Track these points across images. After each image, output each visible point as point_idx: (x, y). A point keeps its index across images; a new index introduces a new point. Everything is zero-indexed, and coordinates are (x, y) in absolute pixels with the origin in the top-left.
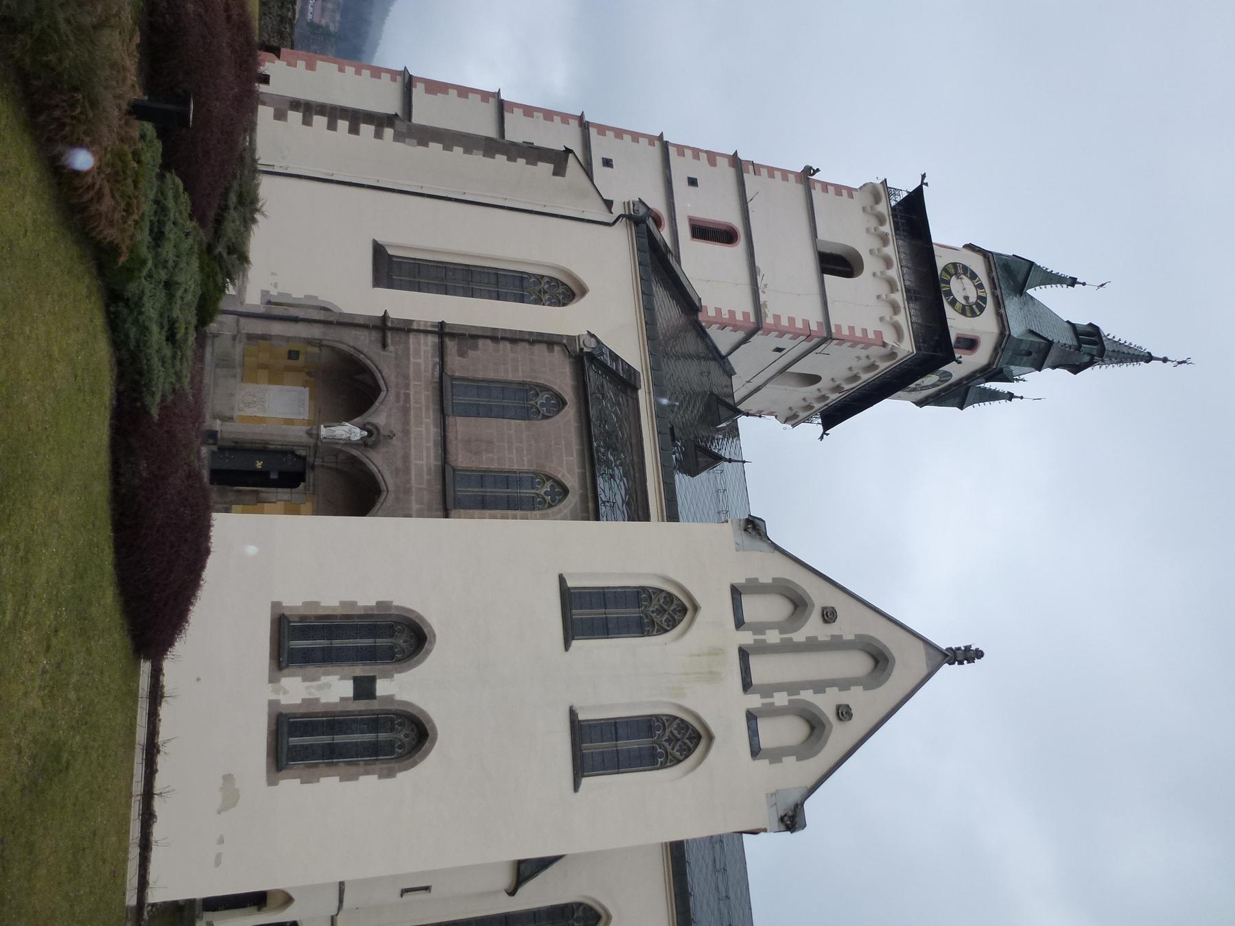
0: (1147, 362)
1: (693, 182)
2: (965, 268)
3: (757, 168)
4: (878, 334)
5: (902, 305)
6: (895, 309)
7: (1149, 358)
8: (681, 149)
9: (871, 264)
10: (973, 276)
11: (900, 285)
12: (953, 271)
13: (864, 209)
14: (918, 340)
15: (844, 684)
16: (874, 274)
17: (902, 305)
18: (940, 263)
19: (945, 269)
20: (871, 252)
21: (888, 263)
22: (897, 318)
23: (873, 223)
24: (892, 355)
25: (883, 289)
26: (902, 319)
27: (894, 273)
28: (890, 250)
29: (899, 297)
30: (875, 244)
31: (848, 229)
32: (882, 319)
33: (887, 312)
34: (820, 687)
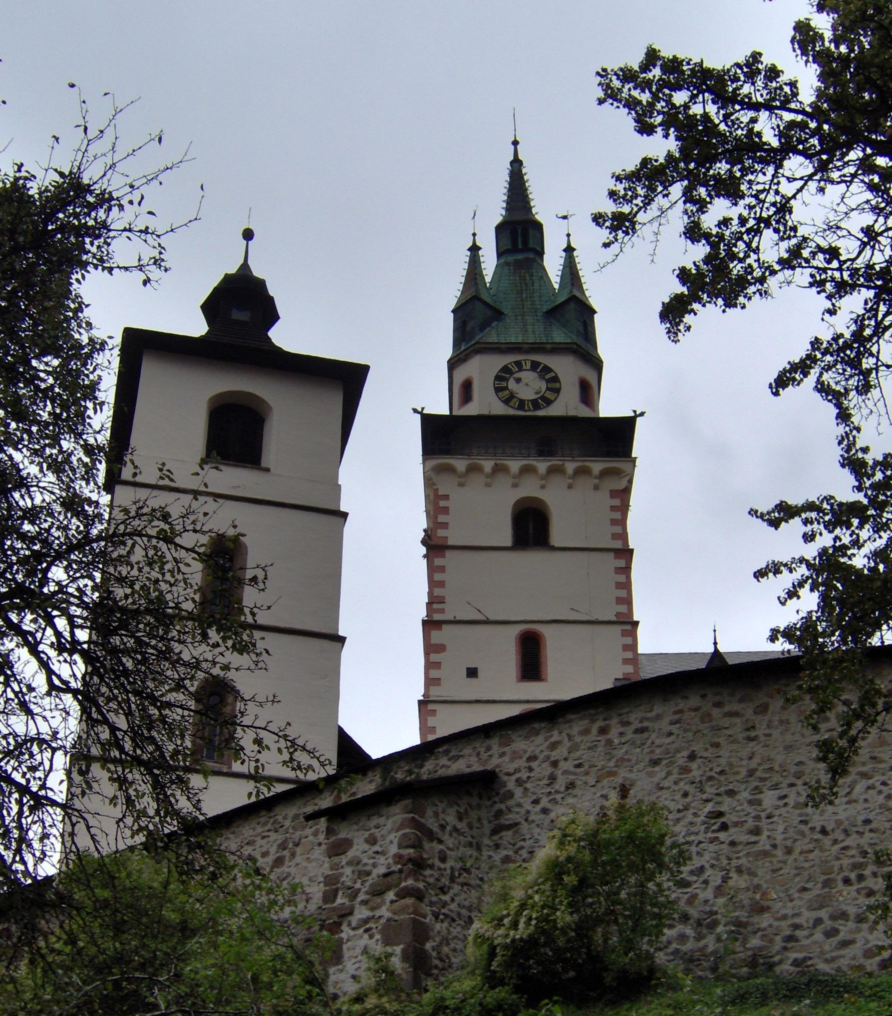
0: (520, 163)
1: (472, 673)
2: (498, 378)
3: (433, 602)
5: (581, 464)
6: (582, 472)
7: (516, 163)
8: (430, 682)
9: (529, 489)
10: (506, 369)
11: (555, 462)
12: (506, 393)
13: (461, 485)
16: (543, 487)
17: (581, 464)
18: (499, 409)
19: (507, 402)
20: (515, 486)
21: (527, 470)
23: (477, 480)
30: (503, 482)
31: (488, 509)
32: (596, 488)
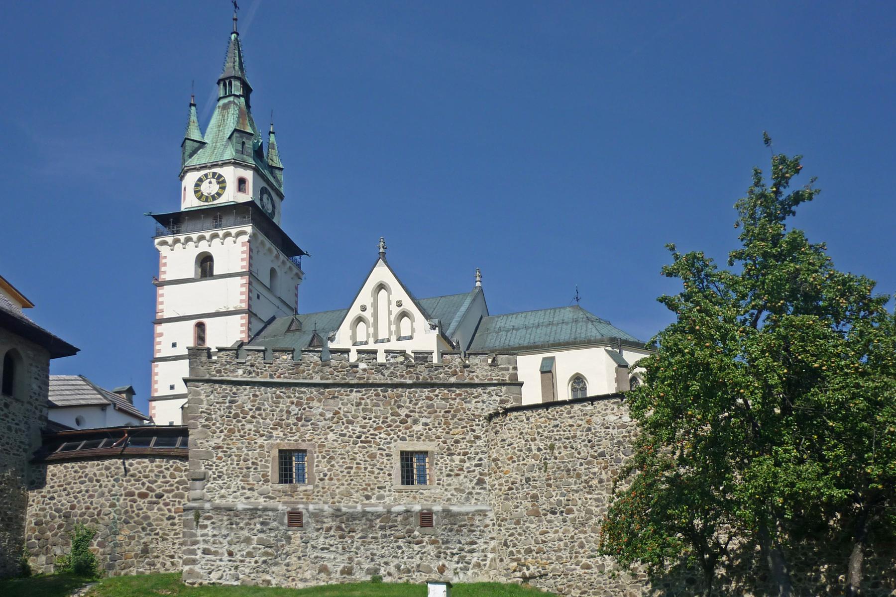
4: (243, 244)
6: (228, 235)
9: (204, 247)
11: (213, 232)
14: (242, 223)
15: (390, 303)
20: (197, 247)
21: (202, 238)
22: (233, 235)
23: (178, 245)
24: (253, 237)
25: (216, 241)
26: (234, 231)
27: (207, 235)
28: (195, 236)
29: (221, 233)
33: (229, 240)
34: (390, 313)
